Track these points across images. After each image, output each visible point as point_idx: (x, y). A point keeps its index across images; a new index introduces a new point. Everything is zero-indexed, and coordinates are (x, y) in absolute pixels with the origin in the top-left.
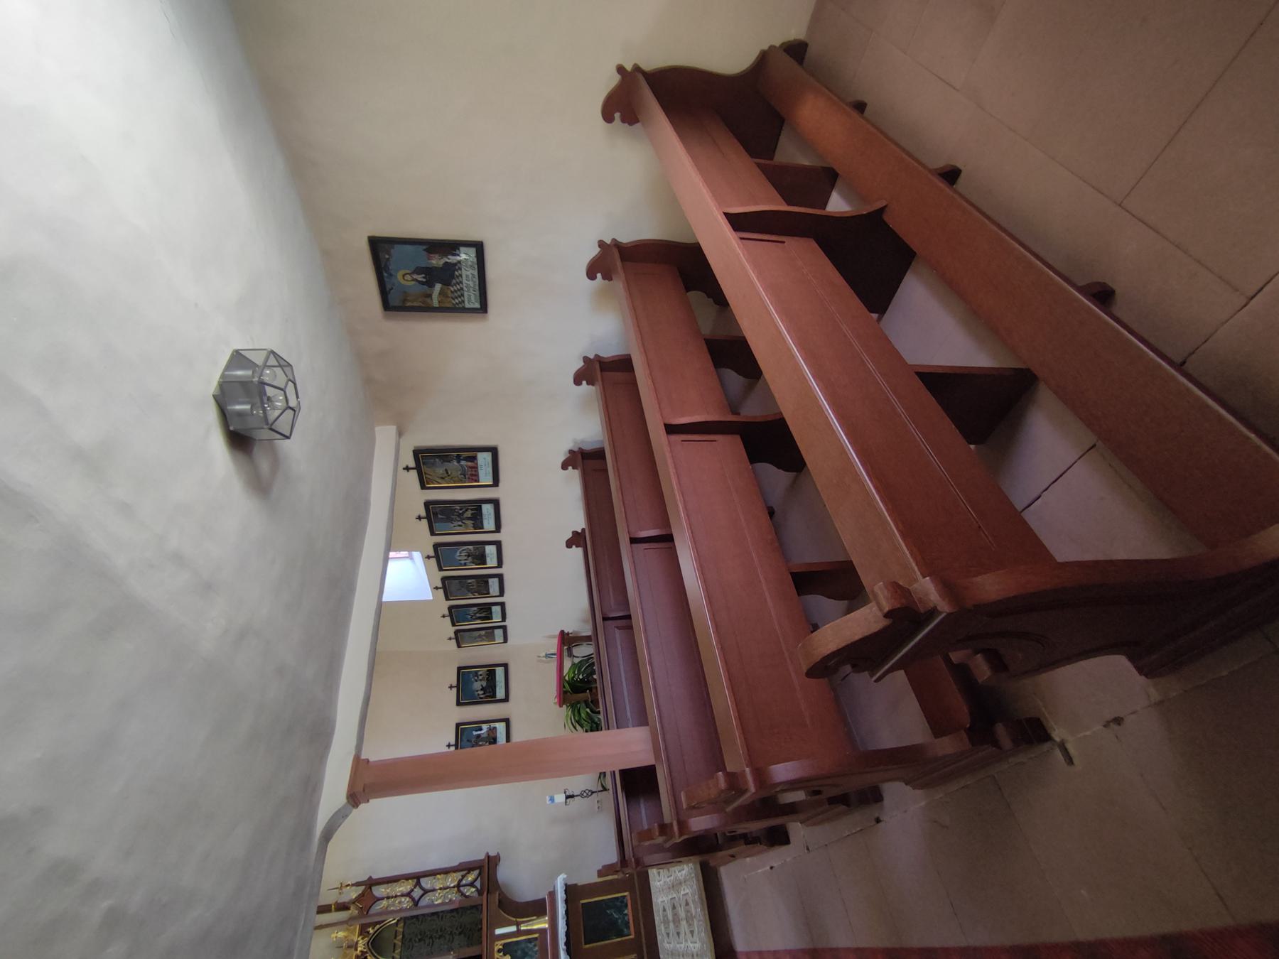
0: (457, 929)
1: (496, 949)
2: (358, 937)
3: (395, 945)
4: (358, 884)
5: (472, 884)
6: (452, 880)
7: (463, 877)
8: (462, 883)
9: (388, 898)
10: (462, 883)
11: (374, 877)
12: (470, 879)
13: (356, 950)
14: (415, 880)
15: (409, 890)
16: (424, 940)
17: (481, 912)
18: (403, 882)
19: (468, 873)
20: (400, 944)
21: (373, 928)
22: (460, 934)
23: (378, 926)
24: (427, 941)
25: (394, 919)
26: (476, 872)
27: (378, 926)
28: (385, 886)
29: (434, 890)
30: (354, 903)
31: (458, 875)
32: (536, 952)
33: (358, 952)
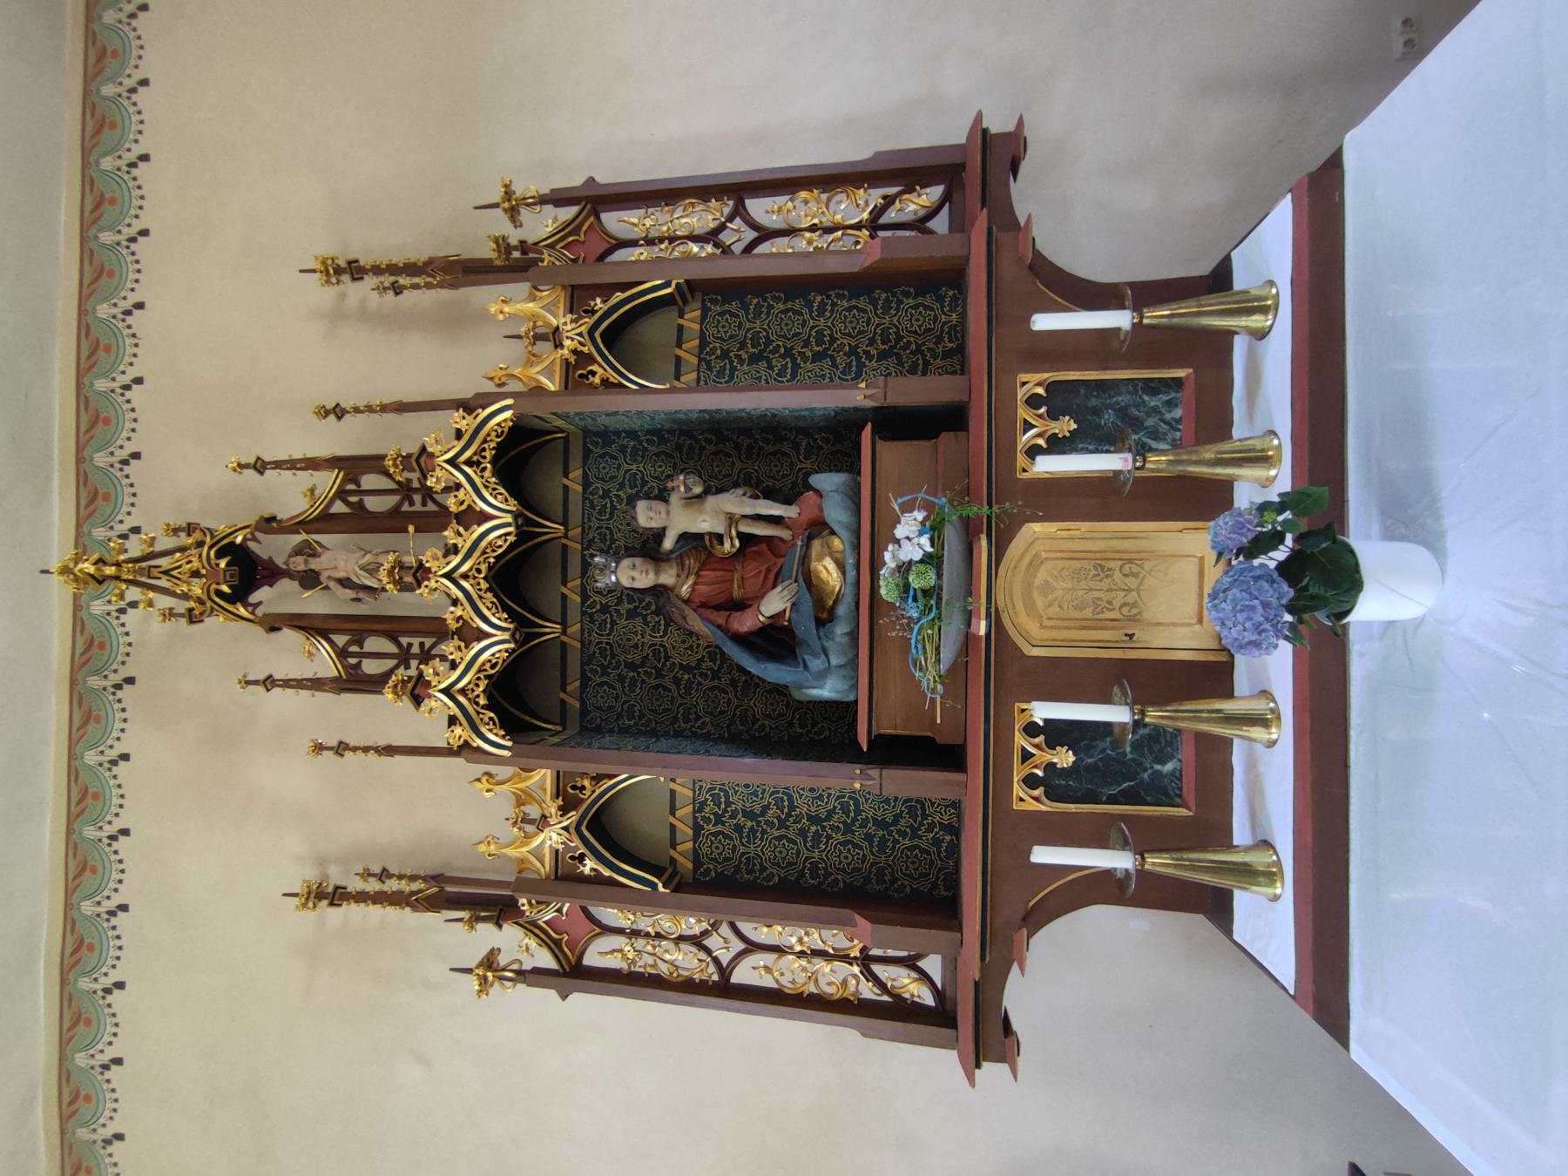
0: (872, 342)
1: (1021, 393)
2: (564, 316)
3: (678, 359)
4: (558, 199)
5: (920, 224)
6: (851, 207)
7: (889, 201)
8: (883, 220)
9: (650, 242)
10: (883, 220)
11: (603, 178)
12: (912, 207)
13: (559, 345)
14: (731, 203)
15: (712, 225)
16: (769, 361)
17: (960, 301)
18: (693, 205)
19: (910, 190)
20: (695, 360)
21: (604, 302)
22: (883, 356)
23: (619, 296)
24: (777, 364)
25: (667, 285)
26: (935, 193)
27: (619, 296)
28: (642, 211)
29: (790, 232)
30: (552, 246)
31: (875, 196)
32: (1173, 425)
33: (566, 352)
